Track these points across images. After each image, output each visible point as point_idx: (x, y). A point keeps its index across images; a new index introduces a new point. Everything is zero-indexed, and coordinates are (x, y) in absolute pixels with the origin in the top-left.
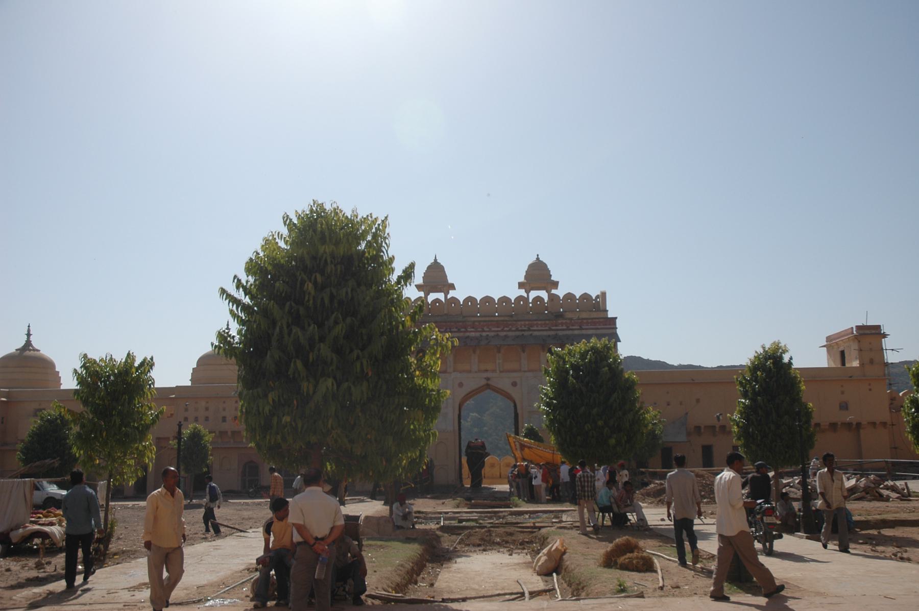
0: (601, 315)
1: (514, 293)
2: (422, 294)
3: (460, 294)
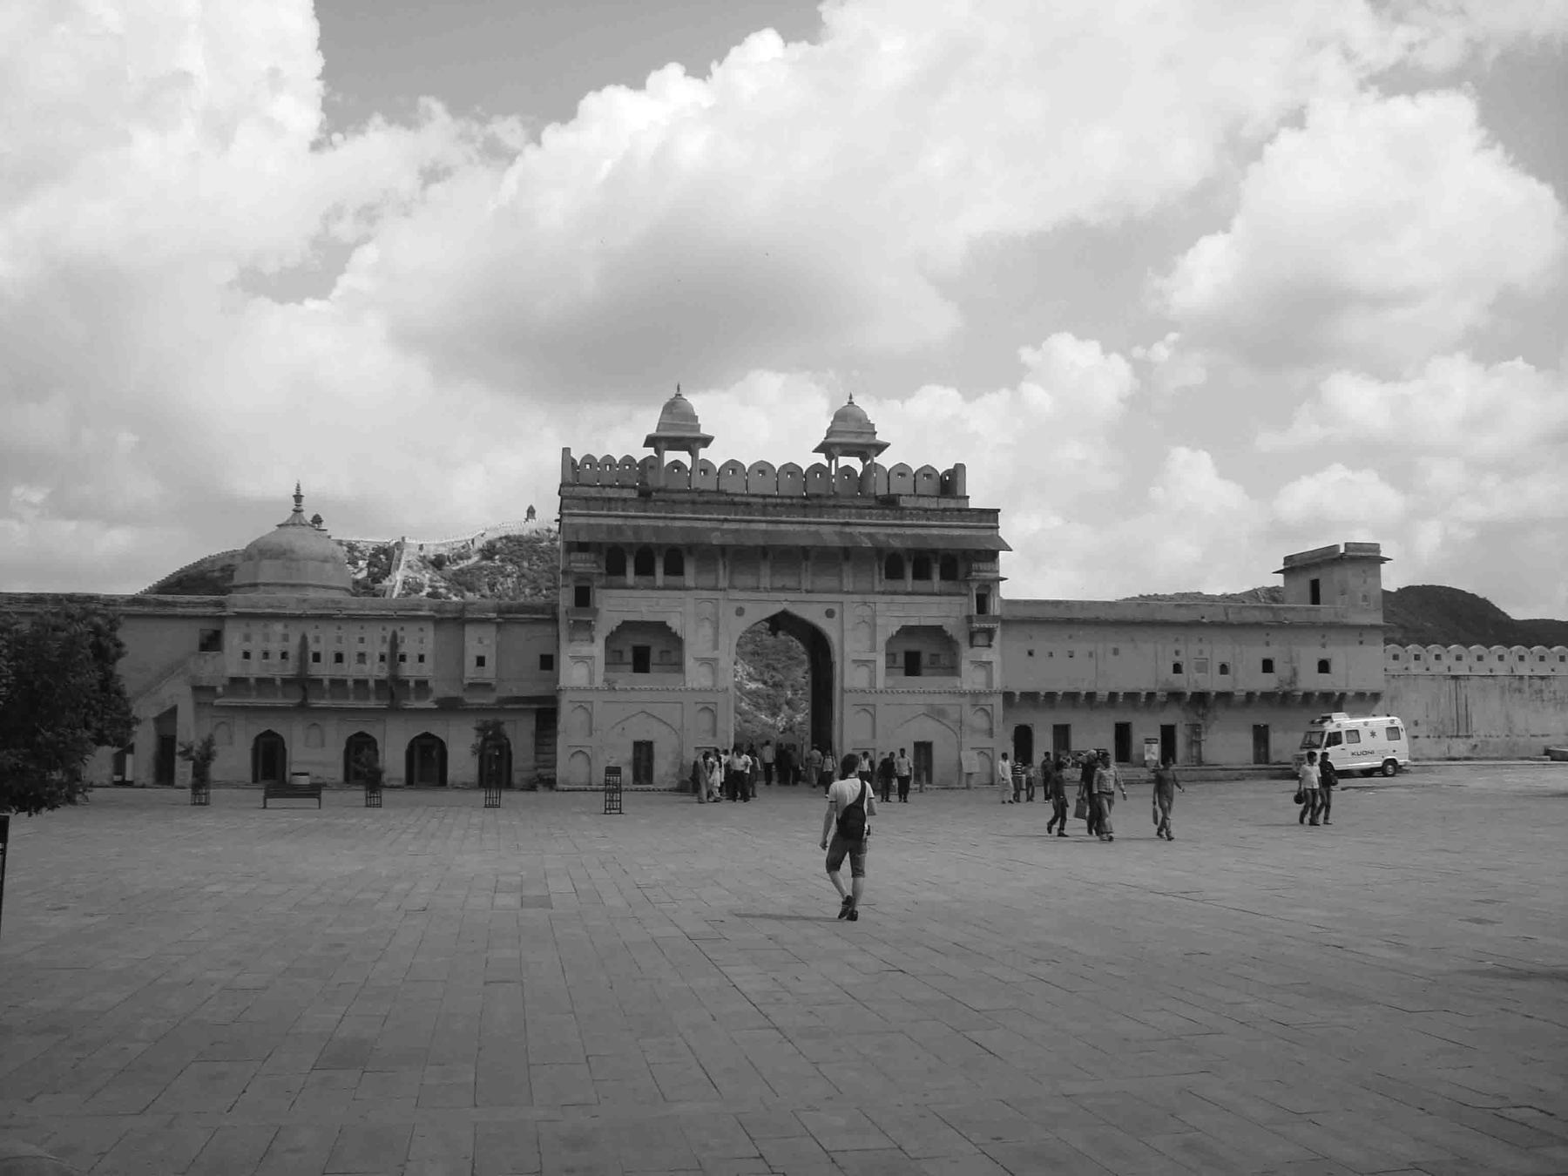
0: (961, 504)
1: (807, 459)
2: (651, 451)
3: (715, 455)
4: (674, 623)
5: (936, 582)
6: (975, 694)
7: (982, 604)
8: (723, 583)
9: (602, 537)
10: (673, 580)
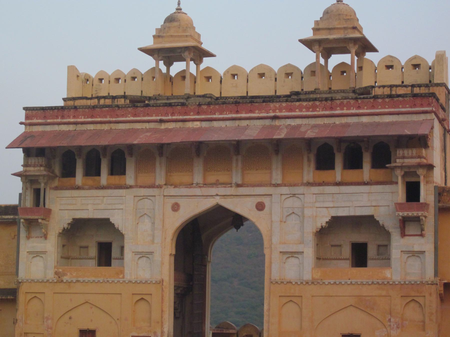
4: (117, 220)
5: (367, 171)
6: (402, 285)
7: (413, 192)
8: (160, 179)
9: (43, 143)
10: (116, 179)
